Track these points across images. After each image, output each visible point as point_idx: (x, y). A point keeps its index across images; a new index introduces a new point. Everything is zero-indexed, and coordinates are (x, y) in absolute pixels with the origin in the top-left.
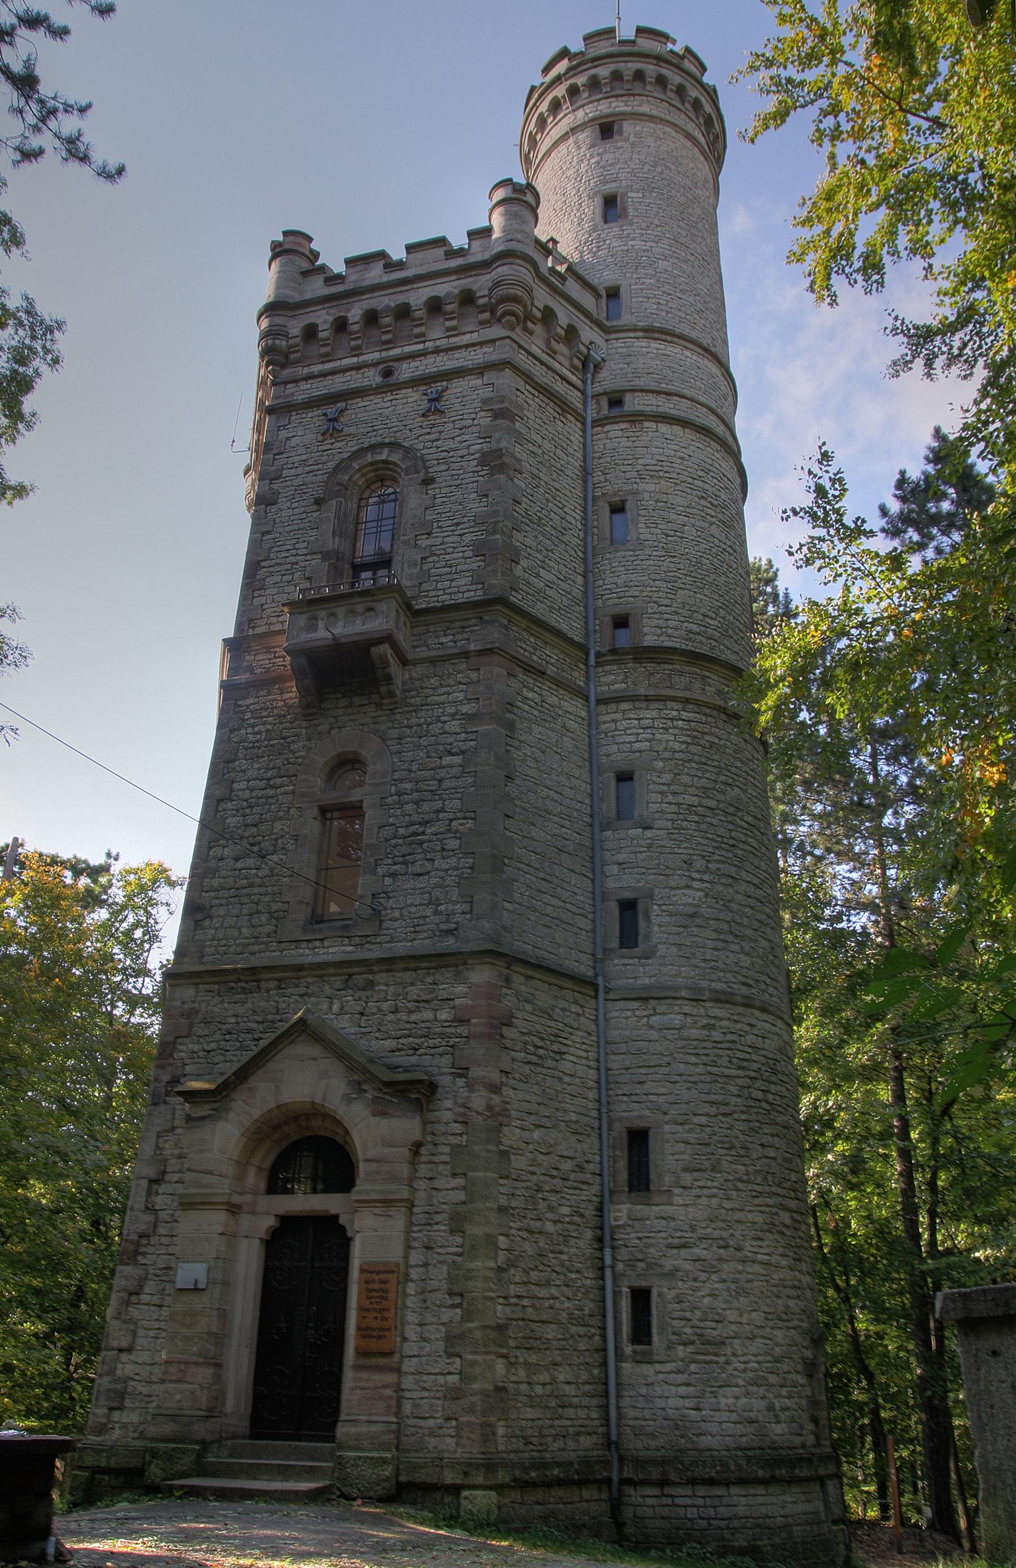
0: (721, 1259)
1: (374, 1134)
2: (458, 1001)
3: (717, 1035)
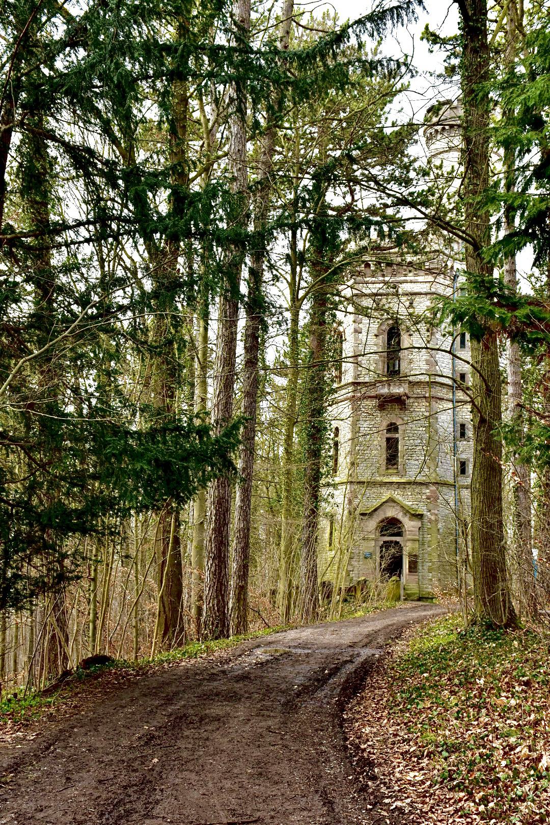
1: (409, 525)
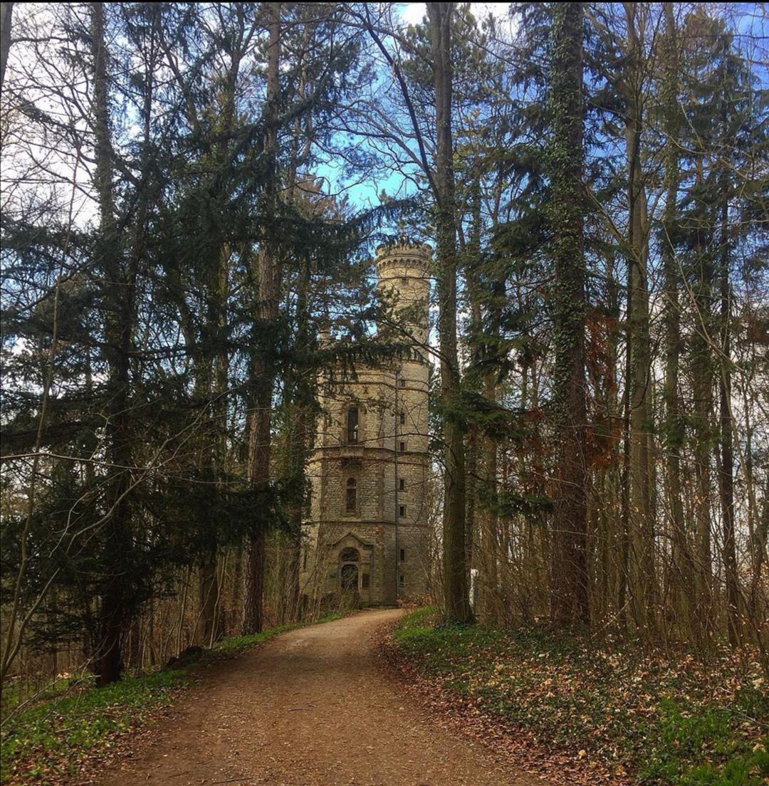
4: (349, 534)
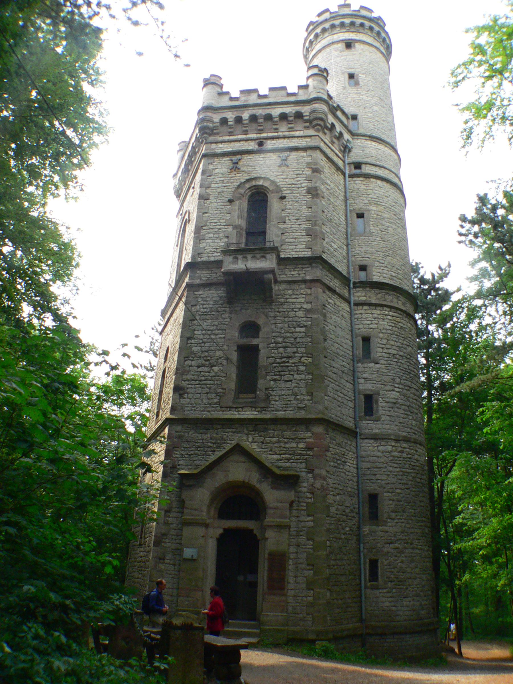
0: (405, 548)
1: (272, 496)
2: (308, 440)
3: (404, 455)
4: (238, 445)
